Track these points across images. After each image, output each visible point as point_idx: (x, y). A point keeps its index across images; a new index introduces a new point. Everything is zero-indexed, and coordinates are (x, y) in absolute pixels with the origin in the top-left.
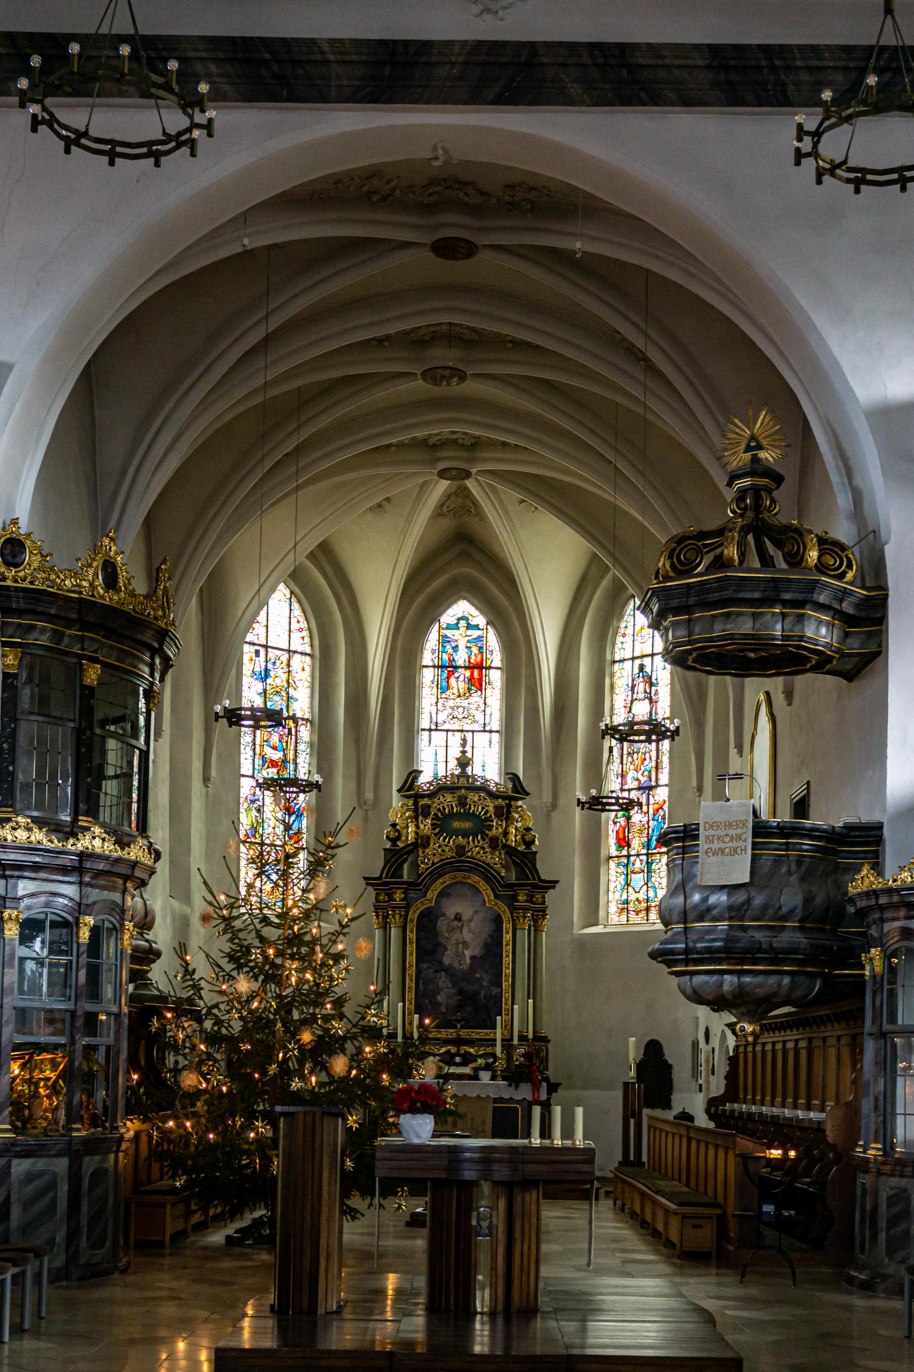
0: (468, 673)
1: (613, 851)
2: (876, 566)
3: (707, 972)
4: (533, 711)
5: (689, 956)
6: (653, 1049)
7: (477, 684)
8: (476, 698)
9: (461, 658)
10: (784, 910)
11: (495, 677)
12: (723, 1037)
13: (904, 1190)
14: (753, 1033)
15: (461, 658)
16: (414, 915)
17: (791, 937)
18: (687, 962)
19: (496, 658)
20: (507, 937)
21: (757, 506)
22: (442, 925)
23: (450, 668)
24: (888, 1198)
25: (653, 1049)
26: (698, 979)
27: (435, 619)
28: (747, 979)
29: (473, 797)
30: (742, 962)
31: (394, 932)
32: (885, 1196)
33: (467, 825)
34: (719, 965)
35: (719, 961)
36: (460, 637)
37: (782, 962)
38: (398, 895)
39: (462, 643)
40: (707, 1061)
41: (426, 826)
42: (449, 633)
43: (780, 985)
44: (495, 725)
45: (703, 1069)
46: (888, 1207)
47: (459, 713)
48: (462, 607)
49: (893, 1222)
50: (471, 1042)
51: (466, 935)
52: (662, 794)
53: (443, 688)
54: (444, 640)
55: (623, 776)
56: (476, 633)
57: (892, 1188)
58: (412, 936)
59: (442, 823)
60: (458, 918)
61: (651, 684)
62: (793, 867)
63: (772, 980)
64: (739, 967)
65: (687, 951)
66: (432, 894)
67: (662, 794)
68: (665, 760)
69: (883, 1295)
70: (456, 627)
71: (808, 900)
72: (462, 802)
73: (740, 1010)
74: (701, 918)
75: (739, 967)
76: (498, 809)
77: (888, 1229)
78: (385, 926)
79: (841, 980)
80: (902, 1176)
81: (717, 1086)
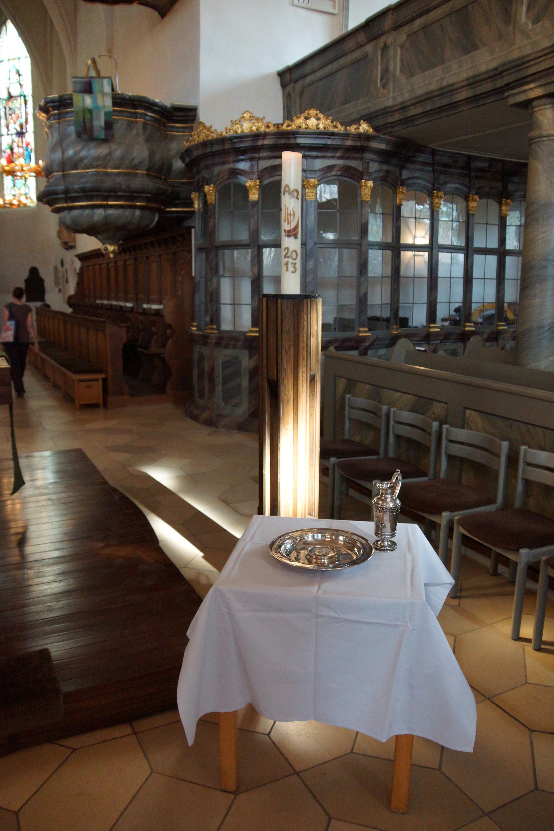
3: (82, 207)
5: (69, 196)
6: (34, 271)
10: (136, 161)
12: (73, 262)
13: (236, 358)
14: (113, 252)
17: (141, 181)
18: (66, 200)
24: (223, 363)
25: (34, 271)
26: (75, 213)
28: (111, 212)
30: (106, 198)
32: (220, 361)
34: (90, 201)
35: (90, 198)
37: (135, 199)
40: (63, 276)
43: (133, 215)
45: (61, 281)
46: (223, 369)
49: (227, 379)
55: (7, 127)
57: (225, 356)
61: (19, 75)
62: (141, 131)
63: (128, 212)
64: (105, 203)
65: (67, 192)
67: (30, 137)
69: (223, 430)
71: (152, 155)
73: (104, 236)
74: (75, 167)
75: (105, 203)
77: (223, 384)
79: (168, 215)
80: (234, 347)
81: (71, 289)
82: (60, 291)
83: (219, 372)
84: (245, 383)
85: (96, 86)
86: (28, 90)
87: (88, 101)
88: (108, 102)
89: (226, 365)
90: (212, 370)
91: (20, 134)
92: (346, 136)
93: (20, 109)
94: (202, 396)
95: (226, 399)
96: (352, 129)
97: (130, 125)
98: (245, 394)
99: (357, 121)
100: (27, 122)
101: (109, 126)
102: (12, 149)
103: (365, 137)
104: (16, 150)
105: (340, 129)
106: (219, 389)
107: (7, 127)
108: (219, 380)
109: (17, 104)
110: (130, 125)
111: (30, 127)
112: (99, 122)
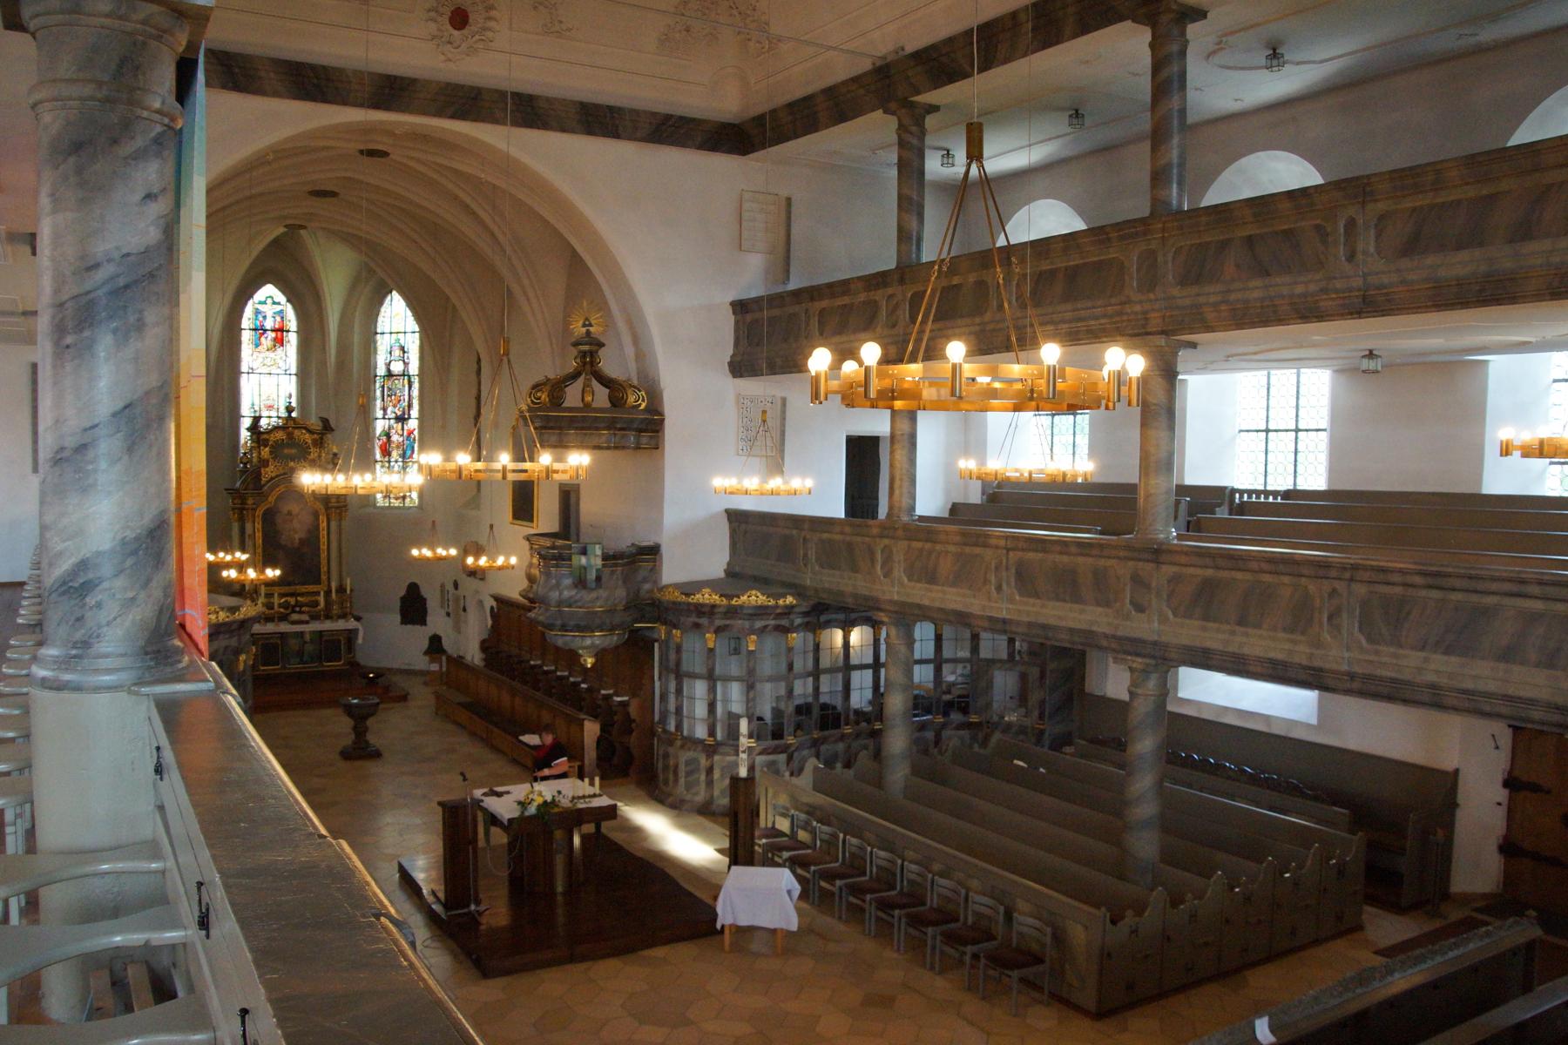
0: (273, 335)
1: (378, 456)
2: (655, 397)
4: (324, 363)
7: (279, 341)
8: (280, 350)
9: (269, 324)
11: (292, 338)
15: (269, 324)
16: (259, 512)
19: (292, 323)
20: (323, 525)
21: (592, 363)
22: (279, 520)
23: (260, 330)
27: (251, 296)
29: (297, 432)
31: (249, 526)
33: (294, 451)
36: (269, 310)
38: (250, 501)
39: (269, 314)
41: (266, 452)
42: (260, 307)
44: (294, 370)
47: (268, 362)
48: (269, 290)
50: (302, 595)
51: (296, 524)
52: (413, 424)
53: (257, 345)
54: (257, 312)
55: (385, 409)
56: (278, 308)
58: (258, 526)
59: (277, 449)
60: (289, 513)
66: (272, 499)
67: (413, 424)
68: (416, 403)
70: (265, 303)
72: (290, 436)
76: (315, 443)
78: (242, 520)
82: (448, 614)
83: (682, 769)
84: (703, 777)
85: (589, 548)
86: (414, 369)
87: (583, 560)
88: (599, 562)
89: (687, 763)
90: (676, 767)
91: (402, 419)
92: (777, 606)
93: (402, 390)
94: (666, 783)
95: (689, 787)
96: (781, 602)
97: (613, 573)
98: (703, 785)
99: (784, 596)
100: (410, 406)
101: (598, 579)
102: (388, 436)
103: (792, 607)
104: (395, 438)
105: (772, 602)
106: (682, 781)
107: (385, 409)
108: (682, 774)
109: (400, 384)
110: (613, 573)
111: (415, 413)
112: (592, 575)
